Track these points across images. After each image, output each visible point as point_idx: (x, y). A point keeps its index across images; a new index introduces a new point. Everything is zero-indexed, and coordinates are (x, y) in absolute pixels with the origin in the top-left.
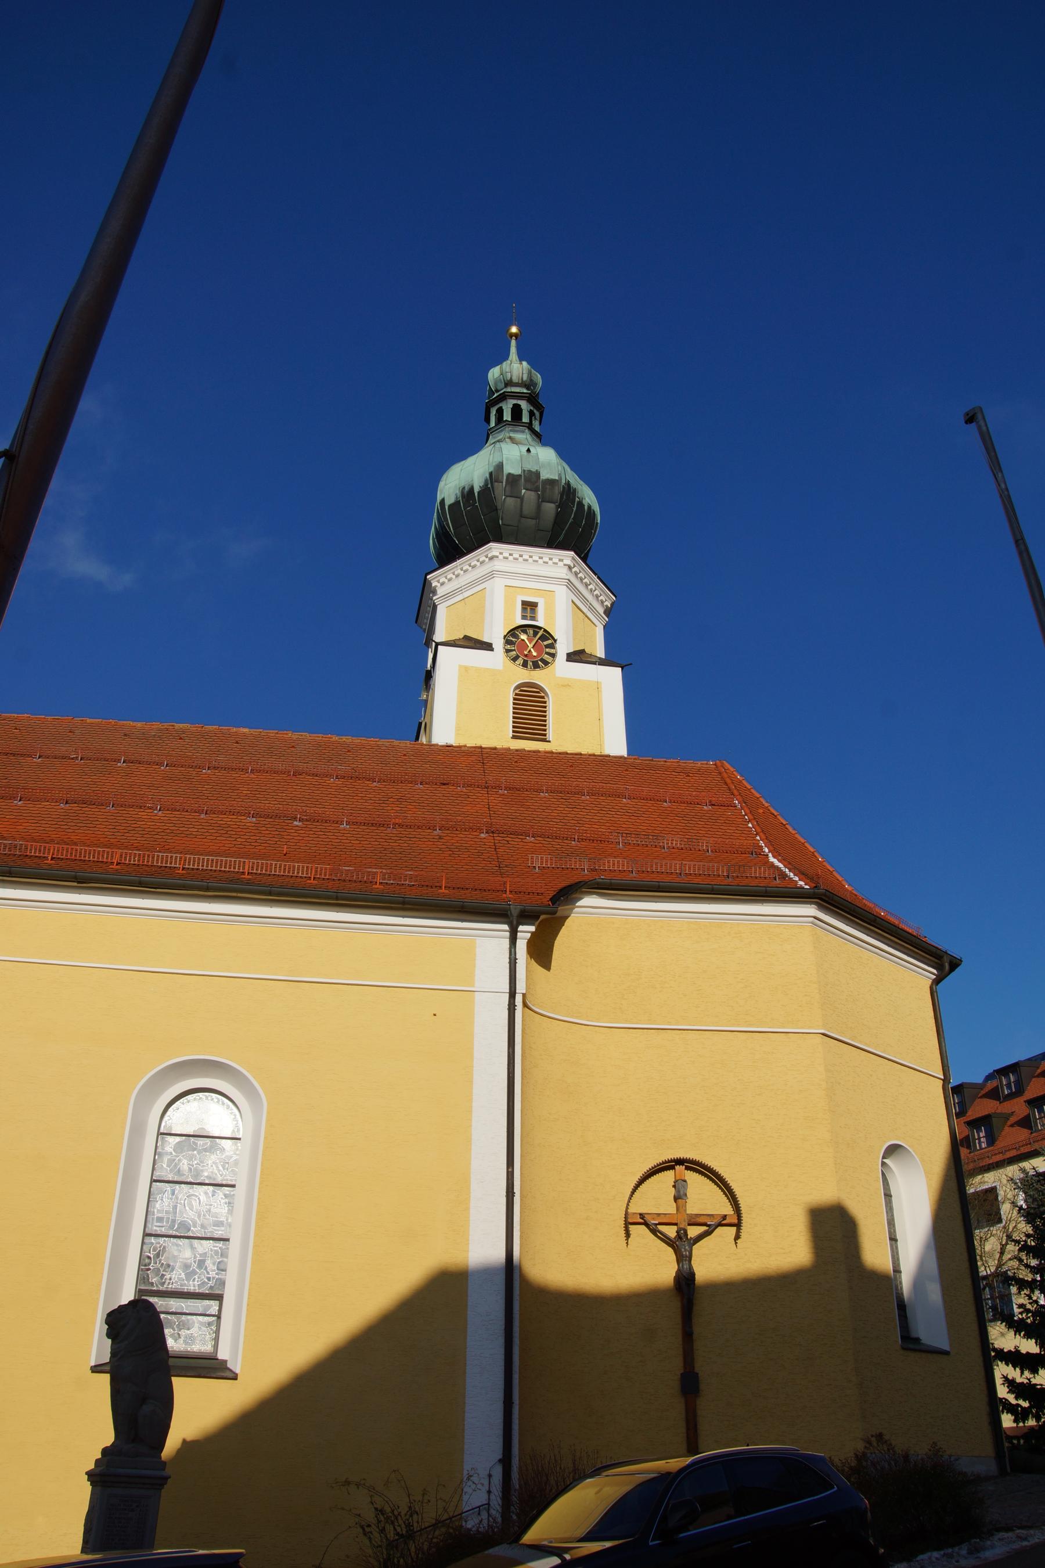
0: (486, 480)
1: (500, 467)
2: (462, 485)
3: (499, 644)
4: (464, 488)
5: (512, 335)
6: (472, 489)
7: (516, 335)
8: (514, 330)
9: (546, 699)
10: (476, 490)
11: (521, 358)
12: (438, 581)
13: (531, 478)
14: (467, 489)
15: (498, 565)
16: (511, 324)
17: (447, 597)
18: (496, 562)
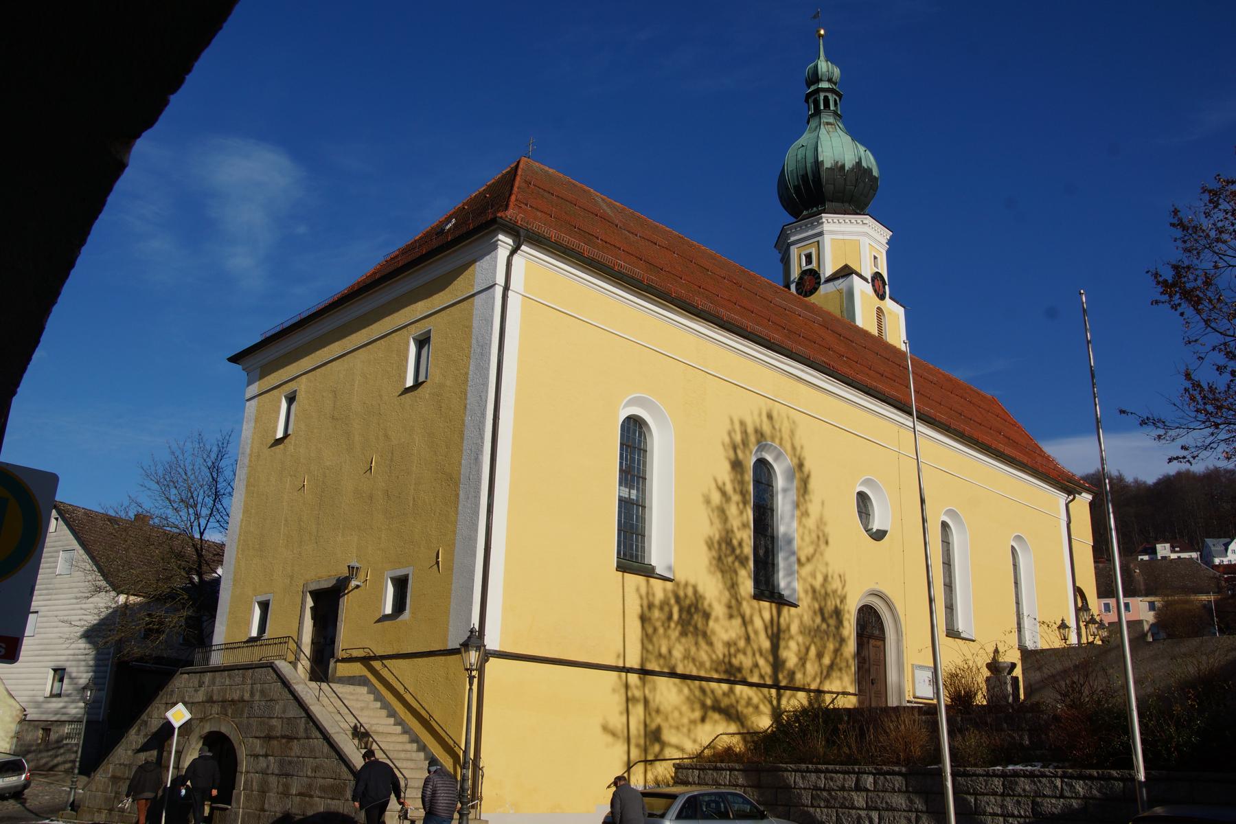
0: (853, 165)
1: (860, 159)
2: (837, 159)
3: (870, 281)
4: (837, 162)
5: (820, 36)
6: (843, 167)
7: (822, 36)
8: (822, 32)
9: (882, 318)
10: (847, 168)
11: (829, 58)
12: (827, 220)
13: (869, 171)
14: (840, 164)
15: (865, 229)
16: (825, 32)
17: (832, 232)
18: (865, 227)
